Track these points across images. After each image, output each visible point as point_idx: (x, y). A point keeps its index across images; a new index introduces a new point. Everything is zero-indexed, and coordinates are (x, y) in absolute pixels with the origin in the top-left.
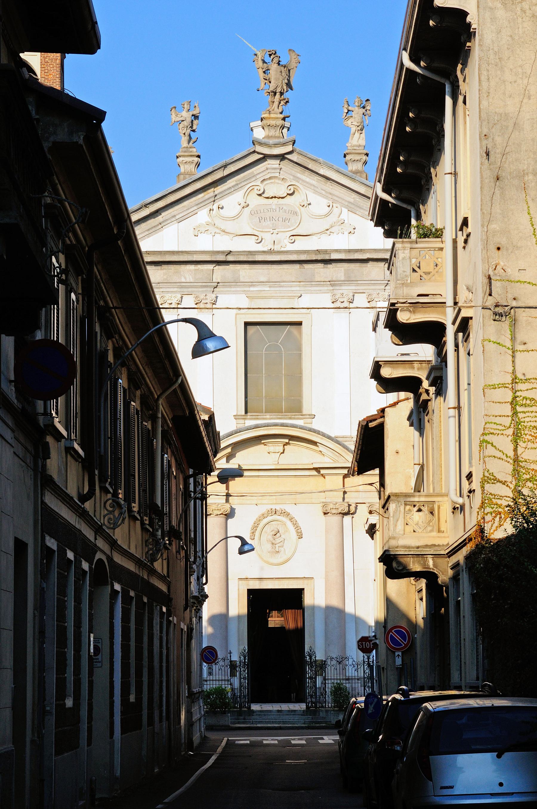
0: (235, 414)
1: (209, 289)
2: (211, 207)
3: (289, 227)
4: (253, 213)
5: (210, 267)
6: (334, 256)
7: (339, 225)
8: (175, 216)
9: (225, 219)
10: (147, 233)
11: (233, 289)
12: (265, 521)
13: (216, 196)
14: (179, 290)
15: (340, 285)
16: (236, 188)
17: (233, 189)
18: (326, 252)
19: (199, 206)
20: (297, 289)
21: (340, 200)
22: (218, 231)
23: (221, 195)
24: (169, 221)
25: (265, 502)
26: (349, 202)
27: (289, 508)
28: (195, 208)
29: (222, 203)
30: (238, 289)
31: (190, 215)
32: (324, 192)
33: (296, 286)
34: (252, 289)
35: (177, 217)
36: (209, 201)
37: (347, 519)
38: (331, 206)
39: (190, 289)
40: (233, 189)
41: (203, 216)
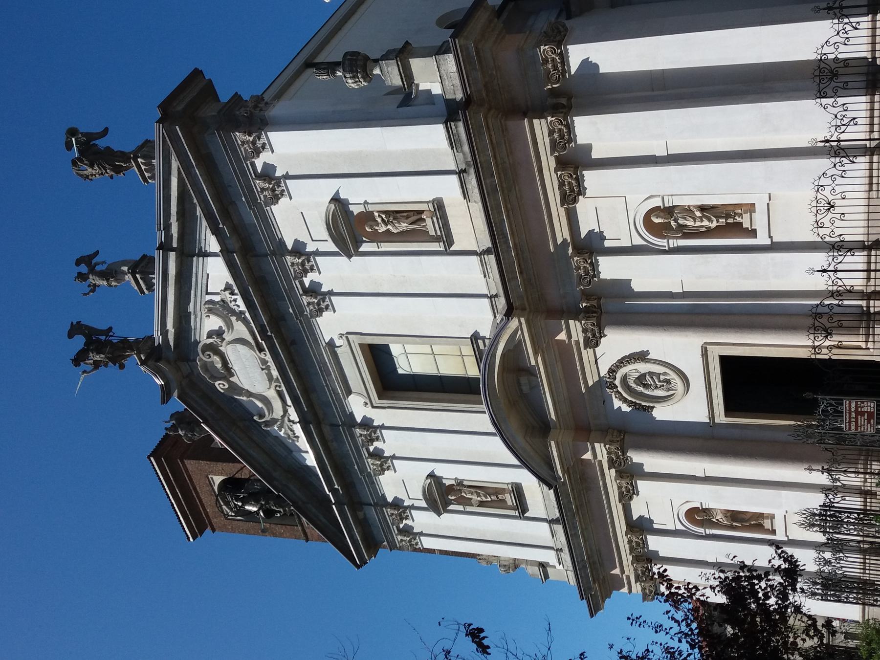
5: (326, 429)
26: (196, 295)
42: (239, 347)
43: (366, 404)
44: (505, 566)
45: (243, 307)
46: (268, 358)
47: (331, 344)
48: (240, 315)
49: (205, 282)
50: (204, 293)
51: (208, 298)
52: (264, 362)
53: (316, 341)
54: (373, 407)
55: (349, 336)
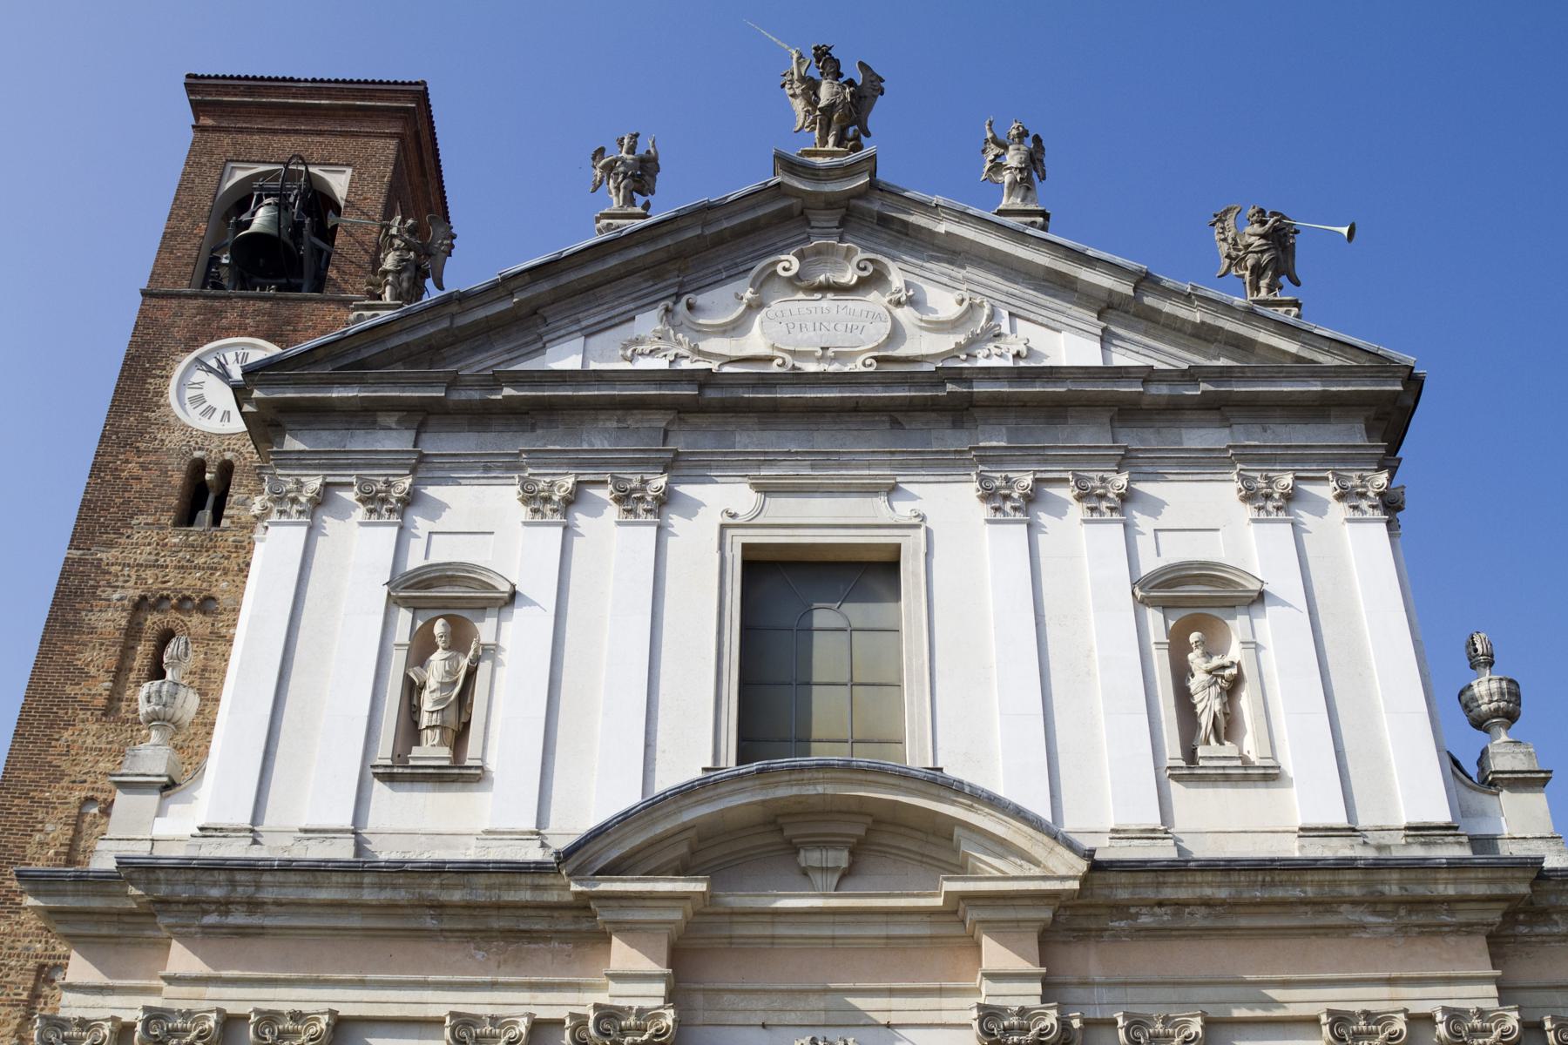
0: (709, 765)
2: (669, 303)
4: (771, 314)
5: (660, 420)
6: (980, 388)
7: (990, 340)
8: (579, 321)
10: (506, 357)
13: (681, 285)
16: (733, 272)
17: (724, 275)
18: (958, 376)
20: (882, 474)
21: (988, 293)
22: (683, 351)
23: (695, 286)
24: (563, 332)
25: (791, 1018)
28: (632, 306)
29: (701, 299)
31: (616, 321)
32: (945, 280)
33: (880, 465)
35: (584, 324)
36: (665, 294)
38: (966, 304)
40: (724, 275)
41: (648, 323)
42: (887, 327)
43: (733, 516)
44: (174, 696)
45: (982, 363)
46: (856, 366)
47: (892, 490)
49: (1032, 316)
50: (1014, 310)
51: (1005, 313)
52: (851, 356)
53: (905, 466)
54: (723, 527)
55: (922, 531)
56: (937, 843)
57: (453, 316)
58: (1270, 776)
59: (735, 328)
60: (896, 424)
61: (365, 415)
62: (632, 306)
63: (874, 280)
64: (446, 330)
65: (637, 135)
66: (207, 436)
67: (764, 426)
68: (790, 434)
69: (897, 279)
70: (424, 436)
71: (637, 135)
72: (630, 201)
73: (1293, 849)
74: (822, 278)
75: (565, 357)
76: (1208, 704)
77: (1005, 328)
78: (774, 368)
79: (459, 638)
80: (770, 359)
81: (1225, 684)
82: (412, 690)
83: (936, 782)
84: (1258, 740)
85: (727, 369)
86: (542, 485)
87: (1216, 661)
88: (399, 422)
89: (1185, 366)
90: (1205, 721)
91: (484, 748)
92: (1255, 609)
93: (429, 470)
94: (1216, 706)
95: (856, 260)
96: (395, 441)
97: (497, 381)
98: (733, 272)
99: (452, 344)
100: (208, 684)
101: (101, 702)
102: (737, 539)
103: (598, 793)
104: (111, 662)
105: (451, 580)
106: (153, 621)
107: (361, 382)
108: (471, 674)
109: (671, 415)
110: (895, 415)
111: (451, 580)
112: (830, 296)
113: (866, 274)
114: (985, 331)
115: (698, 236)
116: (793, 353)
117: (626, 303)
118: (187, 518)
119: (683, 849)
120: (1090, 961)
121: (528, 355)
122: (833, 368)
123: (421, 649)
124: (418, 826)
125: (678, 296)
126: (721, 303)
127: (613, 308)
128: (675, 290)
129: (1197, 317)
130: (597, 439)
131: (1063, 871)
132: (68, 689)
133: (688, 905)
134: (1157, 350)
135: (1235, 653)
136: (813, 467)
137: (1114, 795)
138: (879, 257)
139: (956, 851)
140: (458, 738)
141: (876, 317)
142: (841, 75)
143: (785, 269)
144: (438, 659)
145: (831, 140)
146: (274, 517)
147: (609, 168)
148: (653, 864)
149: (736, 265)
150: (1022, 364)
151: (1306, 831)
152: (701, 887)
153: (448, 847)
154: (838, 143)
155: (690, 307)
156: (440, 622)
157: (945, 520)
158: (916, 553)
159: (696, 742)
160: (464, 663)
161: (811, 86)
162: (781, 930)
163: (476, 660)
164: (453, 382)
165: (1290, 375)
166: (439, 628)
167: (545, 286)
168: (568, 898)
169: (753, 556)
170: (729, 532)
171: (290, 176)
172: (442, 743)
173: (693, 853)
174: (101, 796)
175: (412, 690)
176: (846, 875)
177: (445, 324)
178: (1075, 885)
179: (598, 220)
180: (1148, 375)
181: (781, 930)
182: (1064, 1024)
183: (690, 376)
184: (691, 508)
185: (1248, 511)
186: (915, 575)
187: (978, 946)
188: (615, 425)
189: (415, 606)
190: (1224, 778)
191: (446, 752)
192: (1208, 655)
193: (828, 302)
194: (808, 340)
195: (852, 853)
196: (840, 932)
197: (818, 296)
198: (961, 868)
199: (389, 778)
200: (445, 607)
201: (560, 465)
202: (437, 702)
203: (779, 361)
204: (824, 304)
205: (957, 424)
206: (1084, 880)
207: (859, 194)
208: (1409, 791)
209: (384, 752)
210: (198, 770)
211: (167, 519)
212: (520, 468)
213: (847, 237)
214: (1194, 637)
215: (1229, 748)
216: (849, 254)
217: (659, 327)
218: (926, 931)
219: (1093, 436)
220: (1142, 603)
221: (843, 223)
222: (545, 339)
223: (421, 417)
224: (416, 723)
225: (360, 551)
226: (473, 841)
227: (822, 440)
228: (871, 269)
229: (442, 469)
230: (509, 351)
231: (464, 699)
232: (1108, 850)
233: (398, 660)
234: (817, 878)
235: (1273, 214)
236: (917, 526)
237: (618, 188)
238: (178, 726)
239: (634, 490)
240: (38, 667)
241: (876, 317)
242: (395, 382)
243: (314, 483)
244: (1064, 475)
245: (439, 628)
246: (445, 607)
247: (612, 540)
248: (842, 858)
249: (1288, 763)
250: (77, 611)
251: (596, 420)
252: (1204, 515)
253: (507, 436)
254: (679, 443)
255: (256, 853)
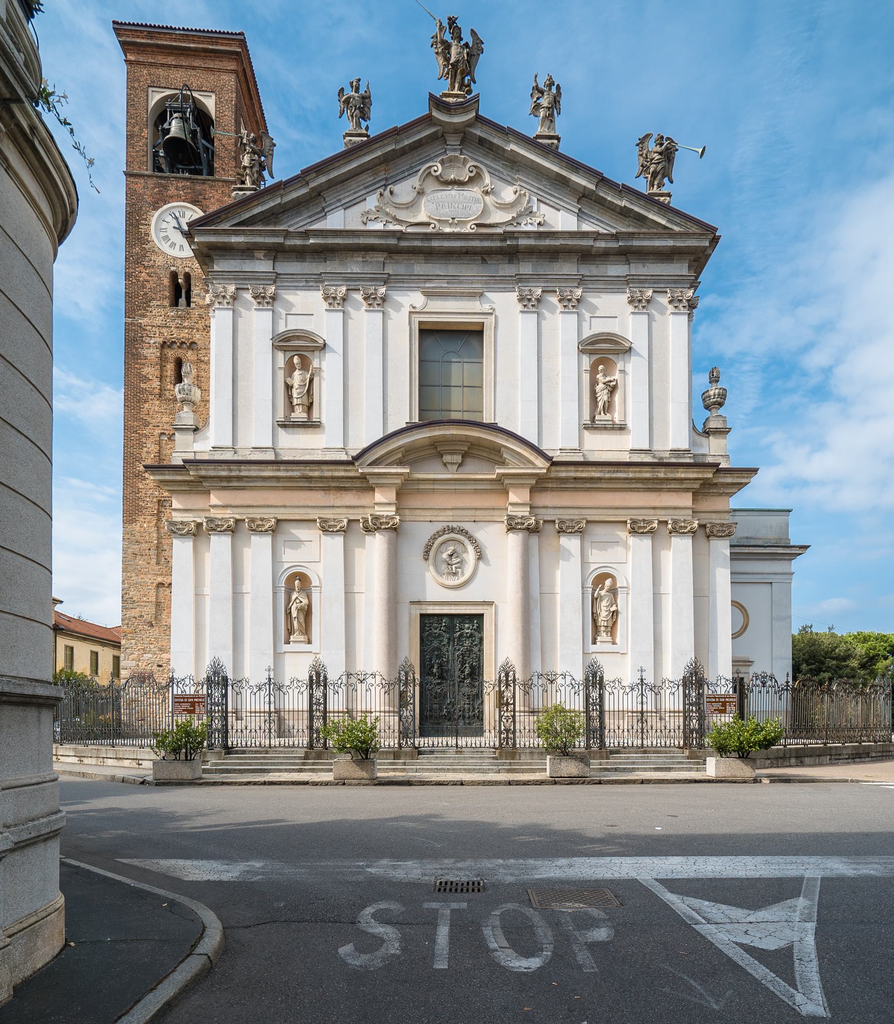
1: (379, 283)
3: (471, 216)
5: (380, 257)
6: (523, 242)
8: (340, 200)
9: (398, 206)
10: (309, 220)
11: (405, 285)
12: (440, 540)
13: (387, 179)
14: (344, 283)
15: (527, 280)
16: (410, 172)
17: (407, 174)
19: (368, 190)
20: (477, 287)
23: (393, 180)
24: (334, 206)
27: (467, 526)
28: (364, 192)
29: (397, 188)
30: (412, 285)
31: (358, 200)
34: (427, 285)
35: (343, 202)
37: (534, 539)
39: (357, 283)
40: (407, 174)
41: (372, 202)
43: (414, 308)
46: (467, 229)
48: (515, 221)
56: (494, 455)
57: (282, 196)
58: (622, 428)
59: (411, 206)
60: (484, 261)
61: (247, 252)
62: (364, 192)
63: (475, 179)
64: (280, 204)
65: (359, 80)
66: (175, 259)
67: (427, 261)
68: (438, 266)
69: (487, 179)
70: (277, 264)
71: (359, 80)
72: (359, 125)
73: (626, 458)
74: (452, 177)
75: (335, 220)
76: (603, 397)
77: (535, 209)
78: (429, 230)
79: (305, 365)
80: (428, 224)
81: (610, 389)
82: (289, 388)
83: (493, 428)
84: (619, 414)
85: (410, 230)
86: (332, 291)
87: (608, 379)
88: (265, 256)
89: (614, 231)
90: (601, 404)
91: (320, 413)
92: (627, 355)
93: (282, 282)
94: (606, 398)
95: (468, 166)
96: (263, 266)
97: (307, 234)
98: (410, 172)
99: (283, 212)
100: (202, 382)
101: (157, 391)
102: (417, 319)
103: (365, 433)
104: (157, 373)
105: (298, 338)
106: (171, 354)
107: (243, 233)
108: (311, 381)
109: (385, 255)
110: (482, 256)
111: (298, 338)
112: (456, 187)
113: (472, 175)
114: (526, 209)
115: (393, 150)
116: (439, 221)
117: (361, 190)
118: (175, 303)
119: (400, 455)
120: (547, 499)
121: (318, 220)
122: (457, 230)
123: (290, 368)
124: (298, 445)
125: (386, 186)
126: (404, 190)
127: (355, 193)
128: (383, 183)
129: (623, 203)
130: (354, 267)
131: (541, 466)
132: (142, 385)
133: (402, 477)
134: (602, 222)
135: (617, 376)
136: (448, 283)
137: (562, 436)
138: (479, 165)
139: (501, 456)
140: (309, 408)
141: (477, 201)
142: (461, 39)
143: (435, 171)
144: (297, 373)
145: (457, 86)
146: (217, 305)
147: (347, 102)
148: (389, 461)
149: (412, 168)
150: (541, 229)
151: (633, 451)
152: (408, 471)
153: (310, 454)
154: (460, 89)
155: (391, 193)
156: (296, 357)
157: (502, 311)
158: (491, 326)
159: (403, 412)
160: (308, 376)
161: (447, 46)
162: (437, 487)
163: (312, 375)
164: (287, 234)
165: (659, 236)
166: (296, 360)
167: (323, 179)
168: (357, 475)
169: (423, 327)
170: (413, 316)
171: (185, 98)
172: (303, 411)
173: (403, 457)
174: (167, 432)
175: (289, 388)
176: (460, 465)
177: (278, 201)
178: (545, 471)
179: (344, 137)
180: (597, 236)
181: (437, 487)
182: (537, 522)
183: (393, 233)
184: (398, 307)
185: (631, 308)
186: (490, 337)
187: (508, 493)
188: (361, 259)
189: (284, 349)
190: (605, 428)
191: (305, 415)
192: (605, 376)
193: (454, 193)
194: (446, 213)
195: (462, 457)
196: (458, 487)
197: (450, 187)
198: (503, 463)
199: (284, 426)
200: (297, 350)
201: (339, 280)
202: (298, 394)
203: (433, 225)
204: (453, 192)
205: (510, 262)
206: (548, 469)
207: (469, 124)
208: (675, 437)
209: (281, 416)
210: (206, 422)
211: (166, 303)
212: (322, 282)
213: (464, 151)
214: (601, 367)
215: (608, 416)
216: (465, 162)
217: (377, 204)
218: (489, 487)
219: (568, 268)
220: (582, 352)
221: (462, 142)
222: (326, 210)
223: (276, 252)
224: (291, 403)
225: (258, 324)
226: (320, 452)
227: (452, 269)
228: (475, 172)
229: (287, 282)
230: (310, 217)
231: (309, 392)
232: (558, 456)
233: (281, 374)
234: (449, 466)
235: (668, 139)
236: (491, 314)
237: (352, 116)
238: (194, 403)
239: (372, 294)
240: (126, 376)
241: (477, 201)
242: (260, 233)
243: (232, 288)
244: (554, 289)
245: (296, 360)
246: (297, 350)
247: (365, 320)
248: (458, 458)
249: (630, 424)
250: (137, 349)
251: (352, 257)
252: (613, 312)
253: (314, 264)
254: (389, 269)
255: (236, 458)
